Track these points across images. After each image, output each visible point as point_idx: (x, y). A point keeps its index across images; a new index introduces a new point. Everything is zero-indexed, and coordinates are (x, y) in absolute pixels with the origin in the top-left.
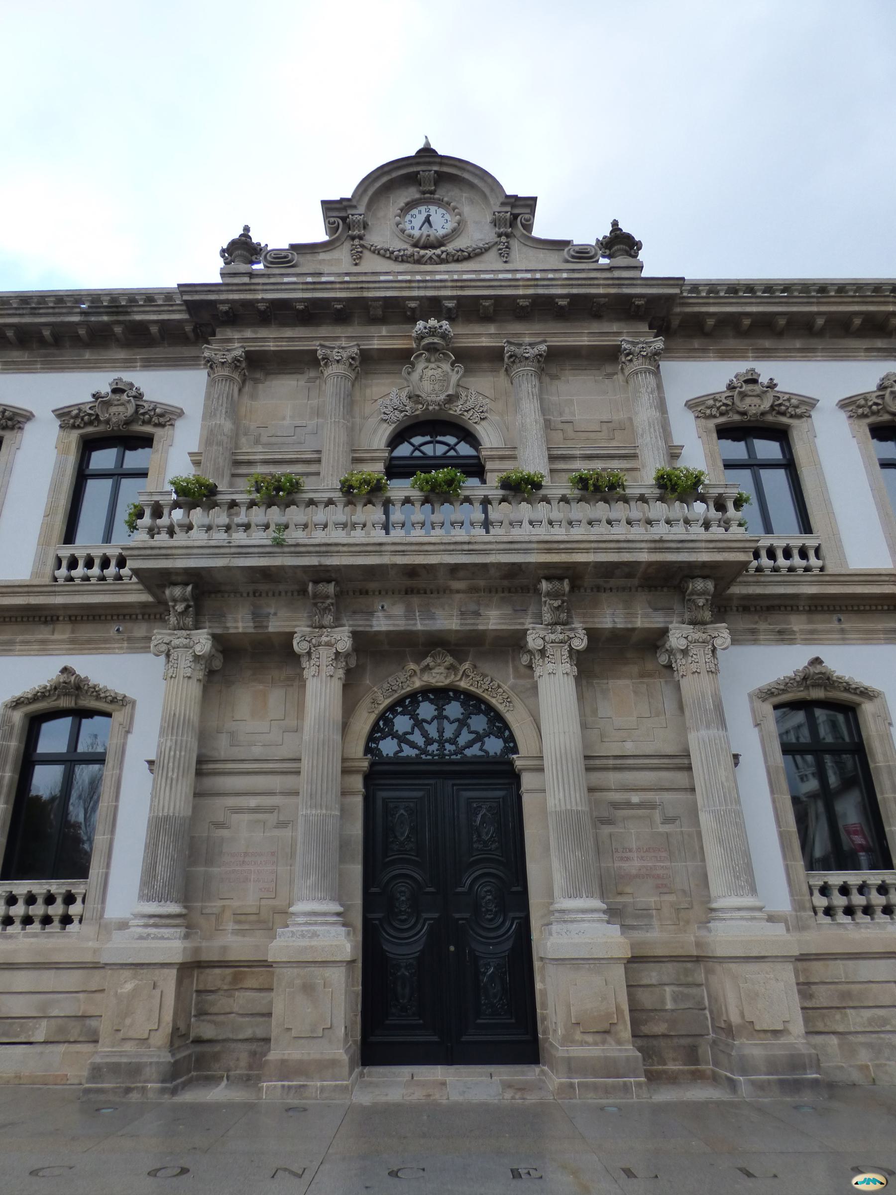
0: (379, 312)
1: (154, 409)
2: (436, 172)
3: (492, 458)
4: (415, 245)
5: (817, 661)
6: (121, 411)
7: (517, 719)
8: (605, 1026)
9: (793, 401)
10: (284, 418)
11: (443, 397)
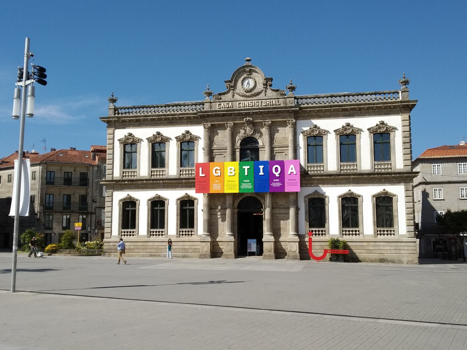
0: (237, 115)
1: (194, 137)
2: (250, 69)
3: (260, 148)
4: (245, 92)
5: (316, 191)
6: (188, 138)
7: (262, 201)
8: (270, 251)
9: (323, 131)
10: (220, 138)
11: (251, 134)
